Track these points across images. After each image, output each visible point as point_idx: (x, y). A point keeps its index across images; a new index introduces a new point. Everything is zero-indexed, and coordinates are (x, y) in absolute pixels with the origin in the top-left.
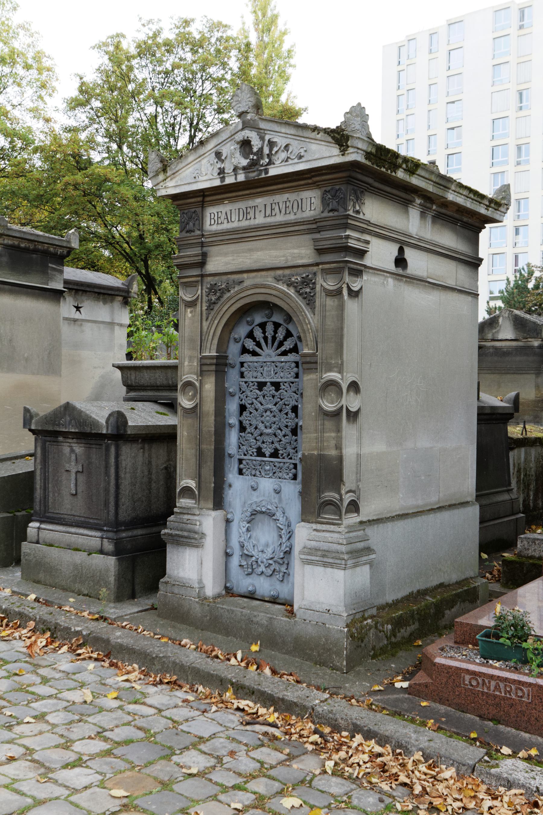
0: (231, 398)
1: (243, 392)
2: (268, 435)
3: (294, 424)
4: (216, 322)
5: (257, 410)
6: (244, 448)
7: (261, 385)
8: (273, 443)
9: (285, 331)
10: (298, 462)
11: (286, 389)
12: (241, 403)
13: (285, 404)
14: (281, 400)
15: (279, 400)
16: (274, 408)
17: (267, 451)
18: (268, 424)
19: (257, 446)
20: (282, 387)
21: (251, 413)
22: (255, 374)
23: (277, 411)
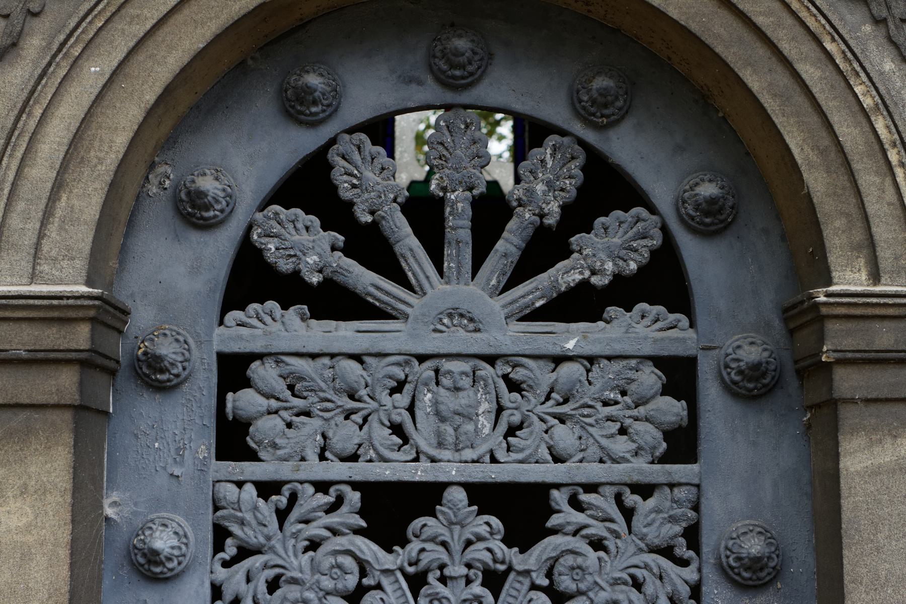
1: (244, 552)
4: (96, 70)
7: (391, 511)
9: (575, 167)
11: (597, 529)
20: (567, 516)
22: (346, 435)
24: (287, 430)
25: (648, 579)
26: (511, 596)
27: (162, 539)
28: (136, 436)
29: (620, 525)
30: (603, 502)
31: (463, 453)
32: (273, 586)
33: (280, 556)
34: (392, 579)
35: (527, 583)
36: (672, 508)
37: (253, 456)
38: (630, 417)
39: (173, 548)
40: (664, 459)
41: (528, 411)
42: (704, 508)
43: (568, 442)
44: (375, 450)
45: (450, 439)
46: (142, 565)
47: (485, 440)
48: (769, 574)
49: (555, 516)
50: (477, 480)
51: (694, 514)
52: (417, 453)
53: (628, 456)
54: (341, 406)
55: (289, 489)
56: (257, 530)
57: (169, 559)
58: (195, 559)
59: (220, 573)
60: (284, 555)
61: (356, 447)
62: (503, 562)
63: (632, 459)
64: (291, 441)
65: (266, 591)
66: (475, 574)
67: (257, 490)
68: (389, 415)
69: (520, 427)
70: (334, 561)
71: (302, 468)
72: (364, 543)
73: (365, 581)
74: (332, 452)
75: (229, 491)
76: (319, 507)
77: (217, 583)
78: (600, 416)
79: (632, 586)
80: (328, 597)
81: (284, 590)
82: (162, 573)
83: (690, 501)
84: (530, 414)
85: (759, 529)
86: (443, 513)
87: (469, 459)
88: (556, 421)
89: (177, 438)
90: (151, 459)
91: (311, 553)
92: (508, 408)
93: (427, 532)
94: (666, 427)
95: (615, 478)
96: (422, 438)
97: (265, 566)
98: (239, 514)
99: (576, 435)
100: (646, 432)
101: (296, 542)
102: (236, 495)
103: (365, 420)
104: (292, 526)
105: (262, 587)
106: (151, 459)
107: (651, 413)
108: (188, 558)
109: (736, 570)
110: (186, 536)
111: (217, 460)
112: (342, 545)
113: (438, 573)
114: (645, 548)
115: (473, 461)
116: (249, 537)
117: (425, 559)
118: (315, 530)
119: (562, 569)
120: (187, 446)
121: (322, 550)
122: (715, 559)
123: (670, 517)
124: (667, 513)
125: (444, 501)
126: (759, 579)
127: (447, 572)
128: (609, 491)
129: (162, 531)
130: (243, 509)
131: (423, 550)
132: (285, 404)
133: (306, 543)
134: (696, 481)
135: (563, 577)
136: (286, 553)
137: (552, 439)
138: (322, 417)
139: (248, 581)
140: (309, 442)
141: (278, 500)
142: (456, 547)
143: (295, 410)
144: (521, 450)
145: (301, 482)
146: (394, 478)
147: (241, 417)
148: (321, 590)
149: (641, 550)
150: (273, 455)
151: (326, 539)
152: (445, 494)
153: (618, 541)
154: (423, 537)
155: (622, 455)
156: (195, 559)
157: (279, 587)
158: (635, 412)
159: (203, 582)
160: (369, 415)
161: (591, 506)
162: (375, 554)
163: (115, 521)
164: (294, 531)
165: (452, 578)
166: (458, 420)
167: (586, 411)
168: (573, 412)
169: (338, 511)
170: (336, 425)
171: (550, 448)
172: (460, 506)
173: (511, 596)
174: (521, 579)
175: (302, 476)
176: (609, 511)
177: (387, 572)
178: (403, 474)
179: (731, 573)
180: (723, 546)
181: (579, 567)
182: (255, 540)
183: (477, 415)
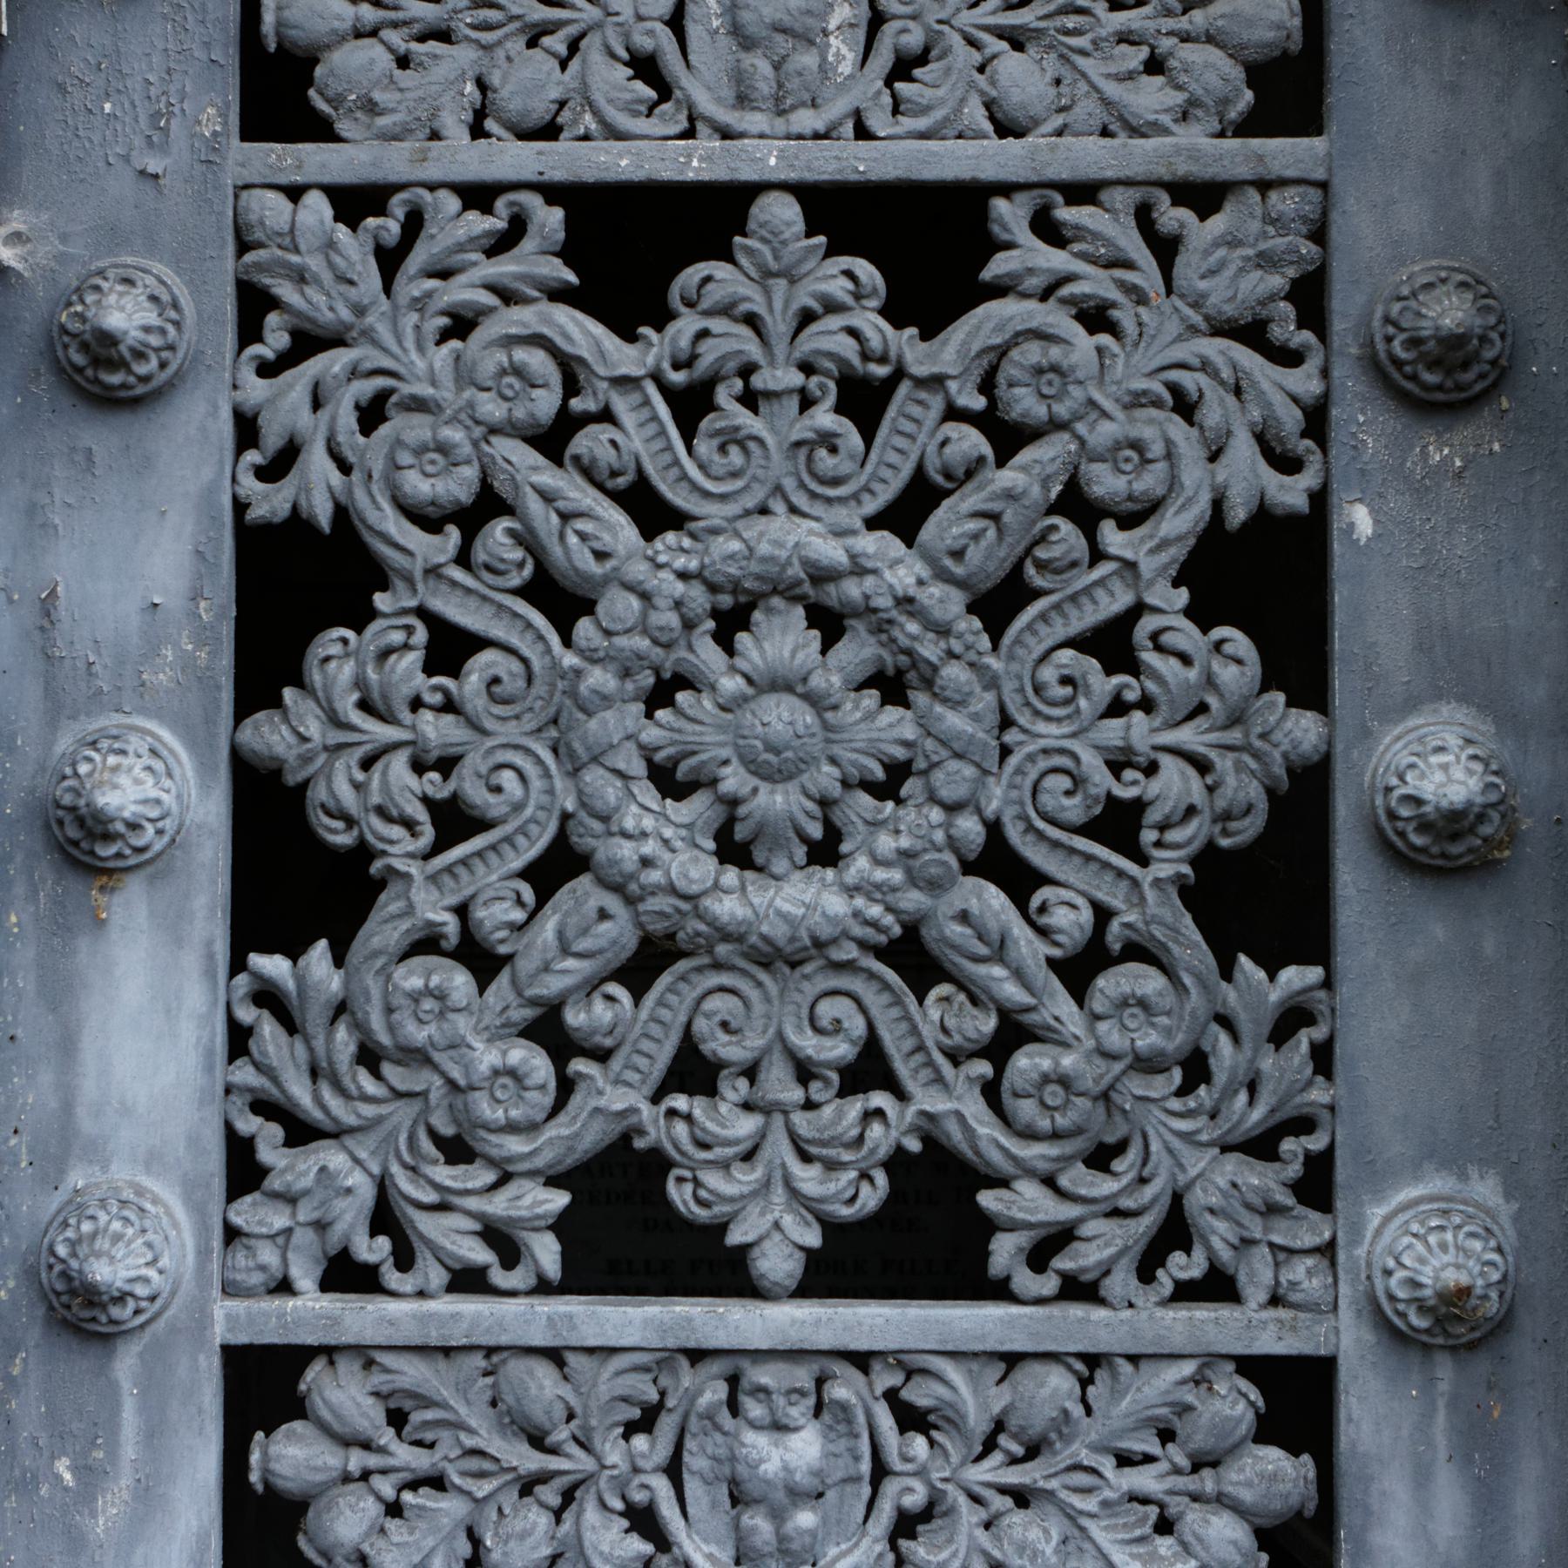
0: (102, 436)
1: (308, 342)
2: (775, 958)
3: (1243, 786)
5: (560, 599)
6: (340, 1176)
7: (633, 247)
8: (869, 1070)
10: (1349, 1340)
11: (1095, 284)
12: (270, 503)
13: (1076, 503)
14: (1008, 438)
15: (970, 441)
16: (898, 568)
17: (769, 1185)
18: (776, 802)
19: (575, 1134)
21: (449, 648)
22: (530, 80)
23: (947, 602)
24: (398, 73)
25: (1208, 394)
26: (900, 433)
27: (122, 309)
28: (62, 88)
29: (1148, 274)
30: (1109, 224)
31: (793, 117)
32: (371, 415)
33: (385, 350)
34: (636, 398)
35: (937, 404)
36: (1265, 235)
37: (323, 131)
38: (1170, 33)
39: (147, 329)
40: (1248, 127)
41: (940, 22)
42: (1335, 235)
43: (1032, 90)
44: (596, 113)
45: (765, 87)
46: (80, 370)
47: (842, 88)
48: (1482, 376)
49: (1000, 256)
50: (825, 177)
51: (1314, 248)
52: (691, 119)
53: (1166, 119)
54: (518, 17)
55: (405, 202)
56: (334, 293)
57: (140, 355)
58: (196, 357)
59: (254, 388)
60: (395, 349)
61: (554, 107)
62: (883, 360)
63: (1174, 128)
64: (409, 95)
65: (356, 427)
66: (822, 387)
67: (334, 206)
68: (627, 36)
69: (922, 59)
70: (505, 359)
71: (433, 154)
72: (573, 319)
73: (576, 404)
74: (499, 120)
75: (272, 209)
76: (472, 240)
77: (247, 409)
78: (1103, 33)
79: (1174, 410)
80: (494, 439)
81: (396, 425)
82: (124, 386)
83: (1304, 219)
84: (945, 28)
85: (1461, 277)
86: (750, 252)
87: (808, 131)
88: (1004, 45)
89: (153, 91)
90: (96, 138)
91: (455, 344)
92: (895, 17)
93: (713, 295)
94: (1252, 55)
95: (1136, 170)
96: (702, 87)
97: (354, 373)
98: (295, 259)
99: (1049, 77)
100: (1206, 65)
101: (422, 319)
102: (287, 217)
103: (574, 46)
104: (410, 285)
105: (348, 420)
106: (96, 138)
107: (1220, 23)
108: (180, 354)
109: (1408, 369)
110: (175, 305)
111: (245, 137)
112: (524, 325)
113: (739, 384)
114: (1203, 326)
115: (817, 136)
116: (317, 309)
117: (709, 354)
118: (463, 292)
119: (1015, 372)
120: (176, 110)
121: (479, 336)
122: (1361, 346)
123: (1260, 254)
124: (1253, 246)
125: (752, 225)
126: (1459, 388)
127: (757, 381)
128: (1121, 199)
129: (121, 295)
130: (303, 247)
131: (704, 334)
132: (392, 15)
133: (444, 321)
134: (1319, 174)
135: (1017, 391)
136: (400, 343)
137: (993, 83)
138: (477, 42)
139: (316, 405)
140: (446, 99)
141: (379, 227)
142: (779, 325)
143: (416, 28)
144: (925, 110)
145: (432, 187)
146: (639, 175)
147: (295, 44)
148: (478, 423)
149: (1193, 330)
150: (369, 127)
151: (488, 311)
152: (754, 210)
153: (1141, 310)
154: (705, 304)
155: (1152, 117)
156: (196, 357)
157: (384, 419)
158: (1183, 23)
159: (216, 407)
160: (583, 35)
161: (1081, 233)
162: (598, 344)
163: (19, 275)
164: (416, 293)
165: (770, 395)
166: (782, 43)
167: (1071, 22)
168: (1042, 24)
169: (516, 251)
170: (509, 59)
171: (989, 105)
172: (787, 235)
173: (900, 433)
174: (923, 395)
175: (433, 172)
176: (1122, 242)
177: (624, 383)
178: (659, 165)
179: (1396, 376)
180: (1379, 314)
181: (1055, 369)
182: (330, 315)
183: (826, 33)
